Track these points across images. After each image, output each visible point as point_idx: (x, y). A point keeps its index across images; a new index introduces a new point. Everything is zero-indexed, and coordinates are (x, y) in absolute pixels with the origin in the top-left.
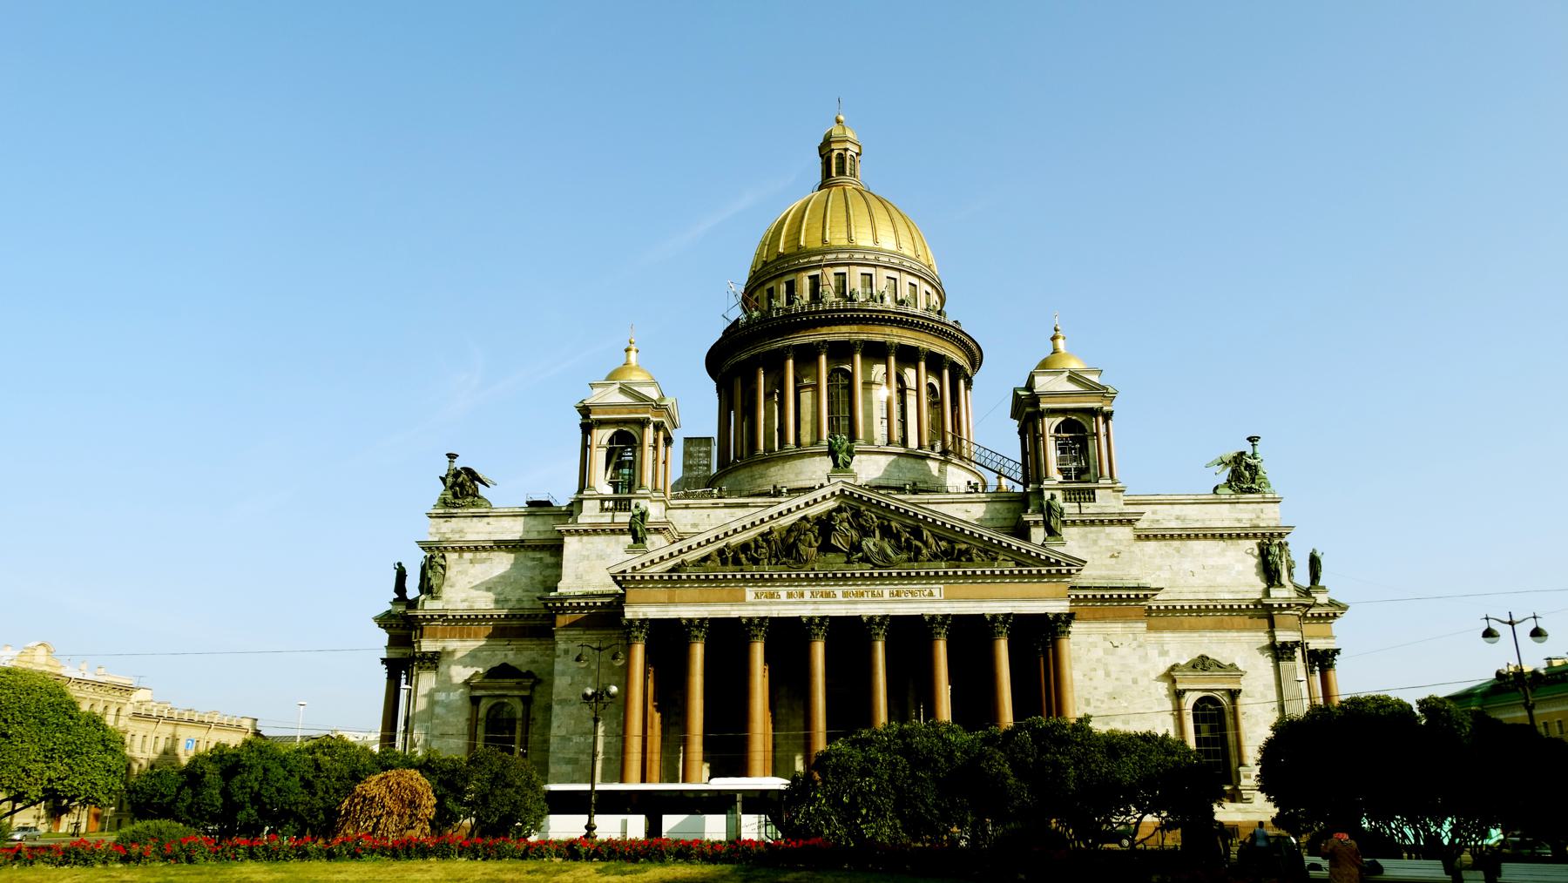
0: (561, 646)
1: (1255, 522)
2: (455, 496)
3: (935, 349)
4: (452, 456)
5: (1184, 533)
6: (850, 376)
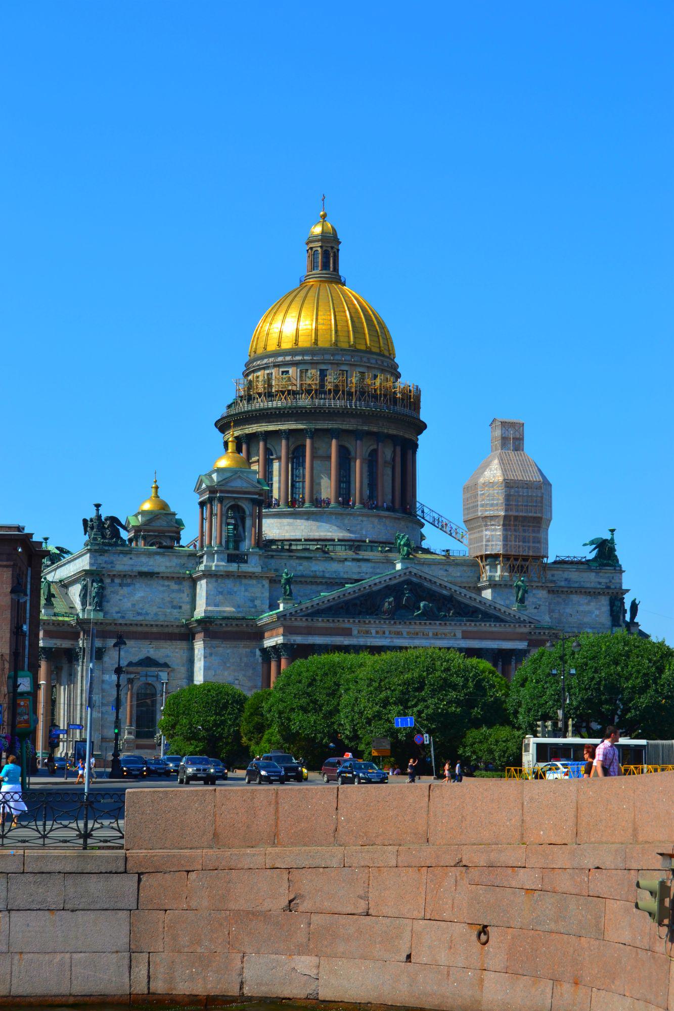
2: (104, 537)
3: (407, 436)
4: (98, 506)
5: (569, 590)
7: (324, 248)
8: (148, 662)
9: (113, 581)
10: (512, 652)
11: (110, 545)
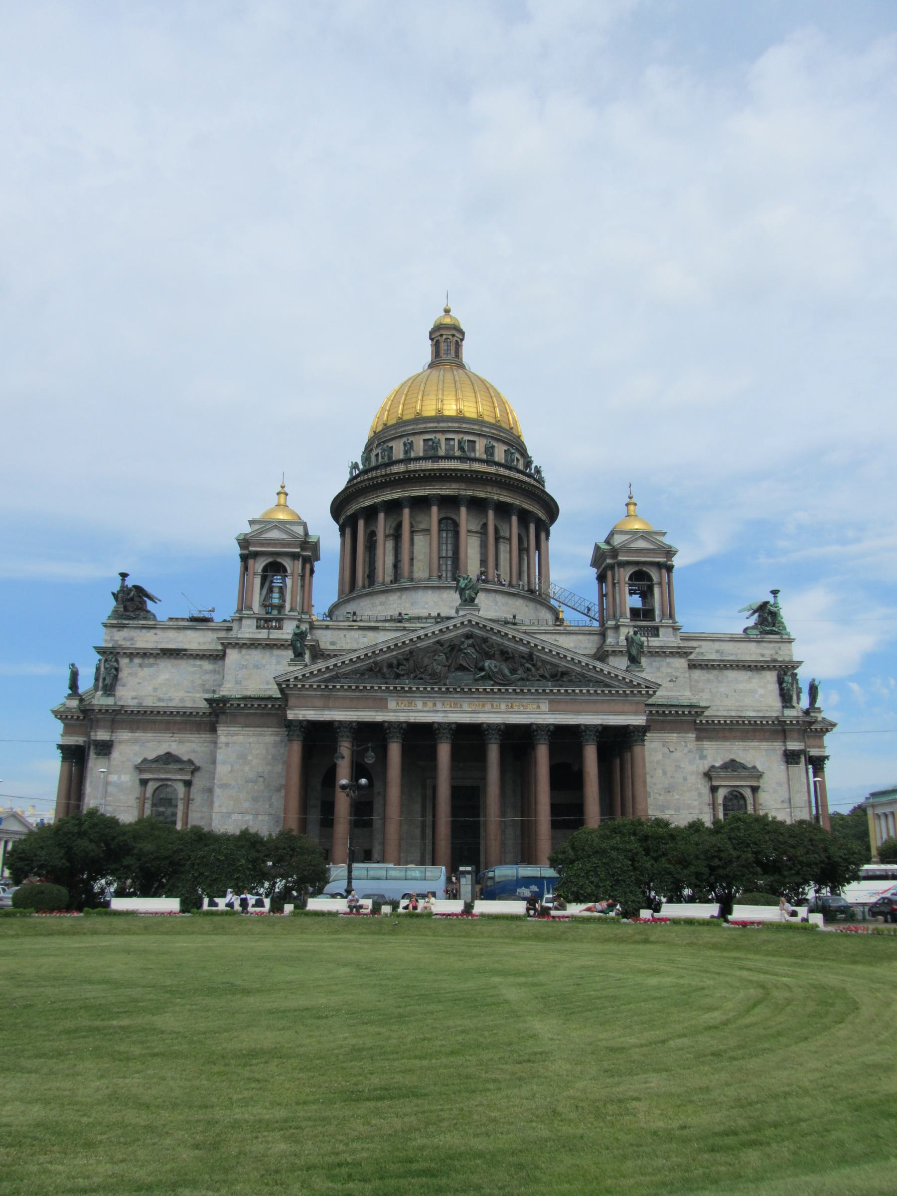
0: (222, 739)
1: (775, 657)
2: (126, 609)
3: (526, 506)
4: (124, 576)
6: (456, 525)
7: (444, 337)
8: (169, 758)
9: (131, 660)
10: (626, 727)
11: (133, 619)
